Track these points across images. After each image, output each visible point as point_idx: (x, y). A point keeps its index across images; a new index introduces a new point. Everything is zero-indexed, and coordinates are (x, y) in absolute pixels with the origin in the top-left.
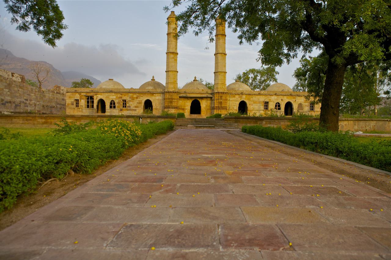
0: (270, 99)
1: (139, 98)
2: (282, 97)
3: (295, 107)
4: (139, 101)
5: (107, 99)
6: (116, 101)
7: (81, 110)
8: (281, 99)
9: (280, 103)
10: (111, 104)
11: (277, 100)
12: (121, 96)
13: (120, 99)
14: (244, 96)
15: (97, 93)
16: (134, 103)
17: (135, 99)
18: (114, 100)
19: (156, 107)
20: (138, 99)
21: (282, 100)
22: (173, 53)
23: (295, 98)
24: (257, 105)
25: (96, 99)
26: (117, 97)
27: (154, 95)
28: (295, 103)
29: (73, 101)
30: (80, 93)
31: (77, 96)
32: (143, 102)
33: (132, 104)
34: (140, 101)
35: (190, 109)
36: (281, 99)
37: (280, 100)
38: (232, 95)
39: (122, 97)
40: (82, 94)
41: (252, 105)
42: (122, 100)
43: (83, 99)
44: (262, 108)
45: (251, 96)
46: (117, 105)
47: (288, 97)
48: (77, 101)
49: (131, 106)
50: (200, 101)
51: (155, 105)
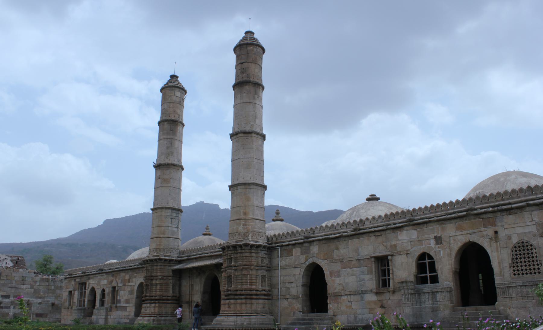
0: (395, 246)
2: (435, 230)
3: (500, 260)
8: (436, 238)
9: (432, 254)
11: (420, 242)
14: (315, 249)
20: (130, 284)
21: (438, 240)
22: (168, 166)
23: (494, 224)
24: (352, 275)
28: (494, 244)
32: (136, 288)
36: (432, 236)
37: (433, 242)
38: (283, 248)
40: (77, 280)
41: (339, 276)
44: (370, 281)
45: (333, 245)
47: (465, 223)
48: (70, 292)
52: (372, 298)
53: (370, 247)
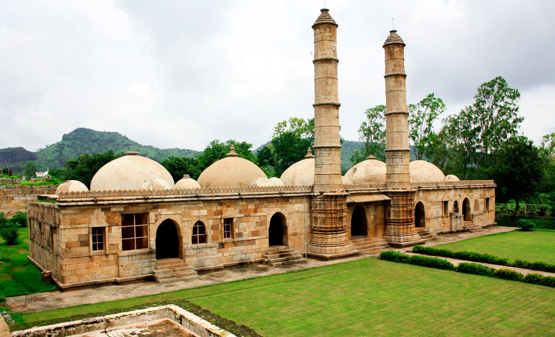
1: (261, 212)
4: (260, 219)
5: (184, 219)
6: (208, 224)
7: (111, 257)
10: (195, 230)
12: (219, 208)
13: (219, 217)
15: (156, 205)
16: (251, 223)
17: (252, 214)
18: (203, 220)
19: (295, 230)
20: (258, 214)
21: (460, 195)
25: (156, 221)
26: (210, 211)
27: (290, 201)
29: (85, 232)
30: (108, 206)
31: (98, 219)
32: (269, 219)
33: (245, 228)
34: (263, 218)
35: (350, 226)
39: (221, 212)
40: (113, 209)
42: (224, 219)
43: (117, 225)
44: (441, 212)
45: (428, 193)
46: (210, 233)
49: (244, 233)
50: (365, 207)
51: (293, 225)
52: (440, 219)
53: (441, 196)
